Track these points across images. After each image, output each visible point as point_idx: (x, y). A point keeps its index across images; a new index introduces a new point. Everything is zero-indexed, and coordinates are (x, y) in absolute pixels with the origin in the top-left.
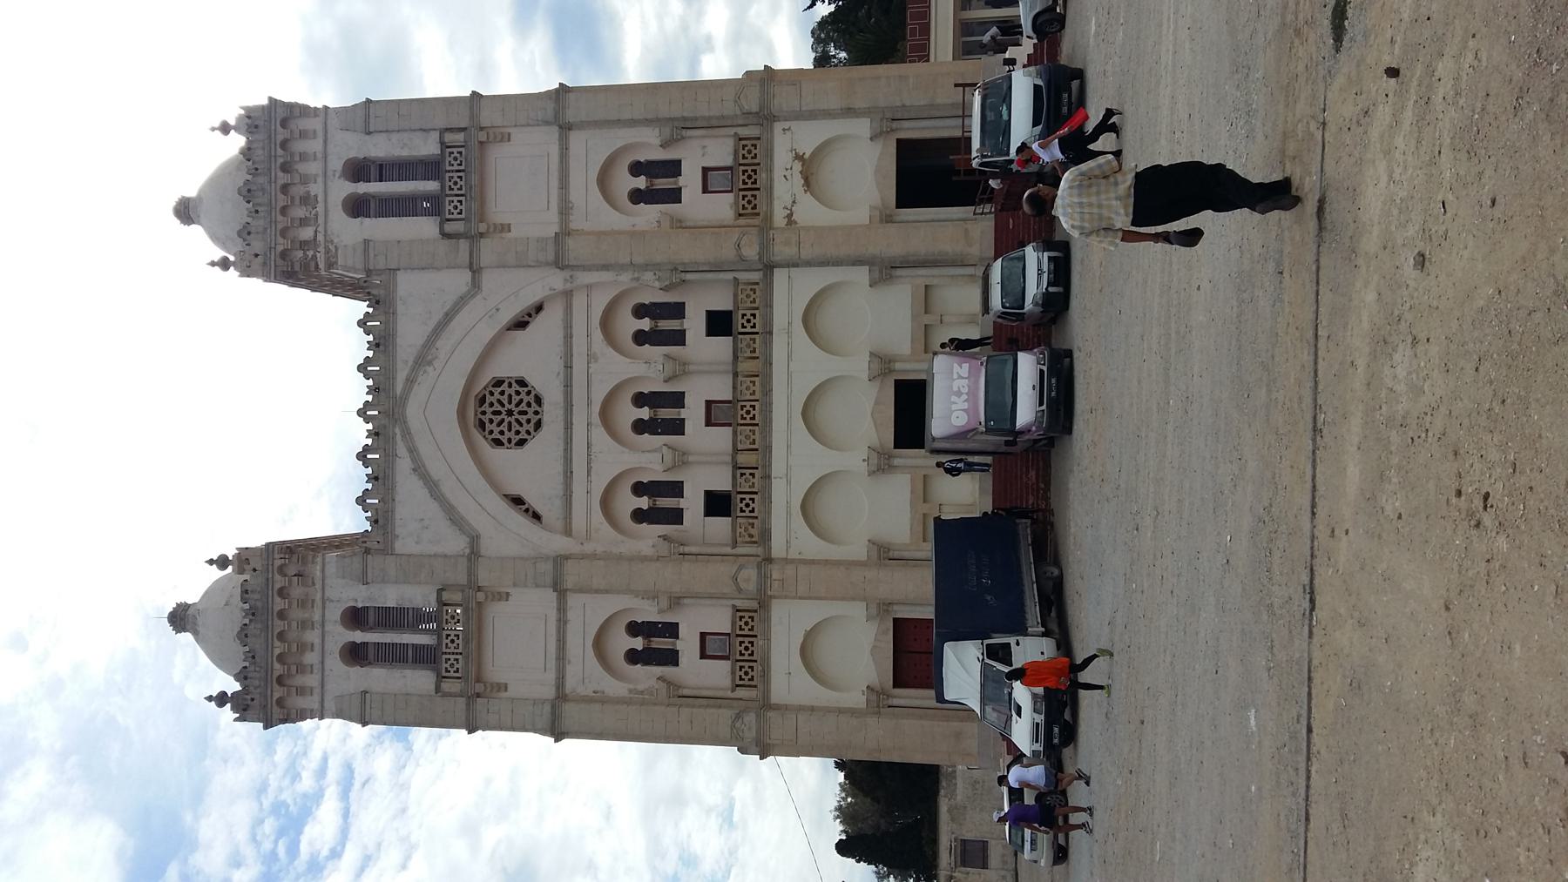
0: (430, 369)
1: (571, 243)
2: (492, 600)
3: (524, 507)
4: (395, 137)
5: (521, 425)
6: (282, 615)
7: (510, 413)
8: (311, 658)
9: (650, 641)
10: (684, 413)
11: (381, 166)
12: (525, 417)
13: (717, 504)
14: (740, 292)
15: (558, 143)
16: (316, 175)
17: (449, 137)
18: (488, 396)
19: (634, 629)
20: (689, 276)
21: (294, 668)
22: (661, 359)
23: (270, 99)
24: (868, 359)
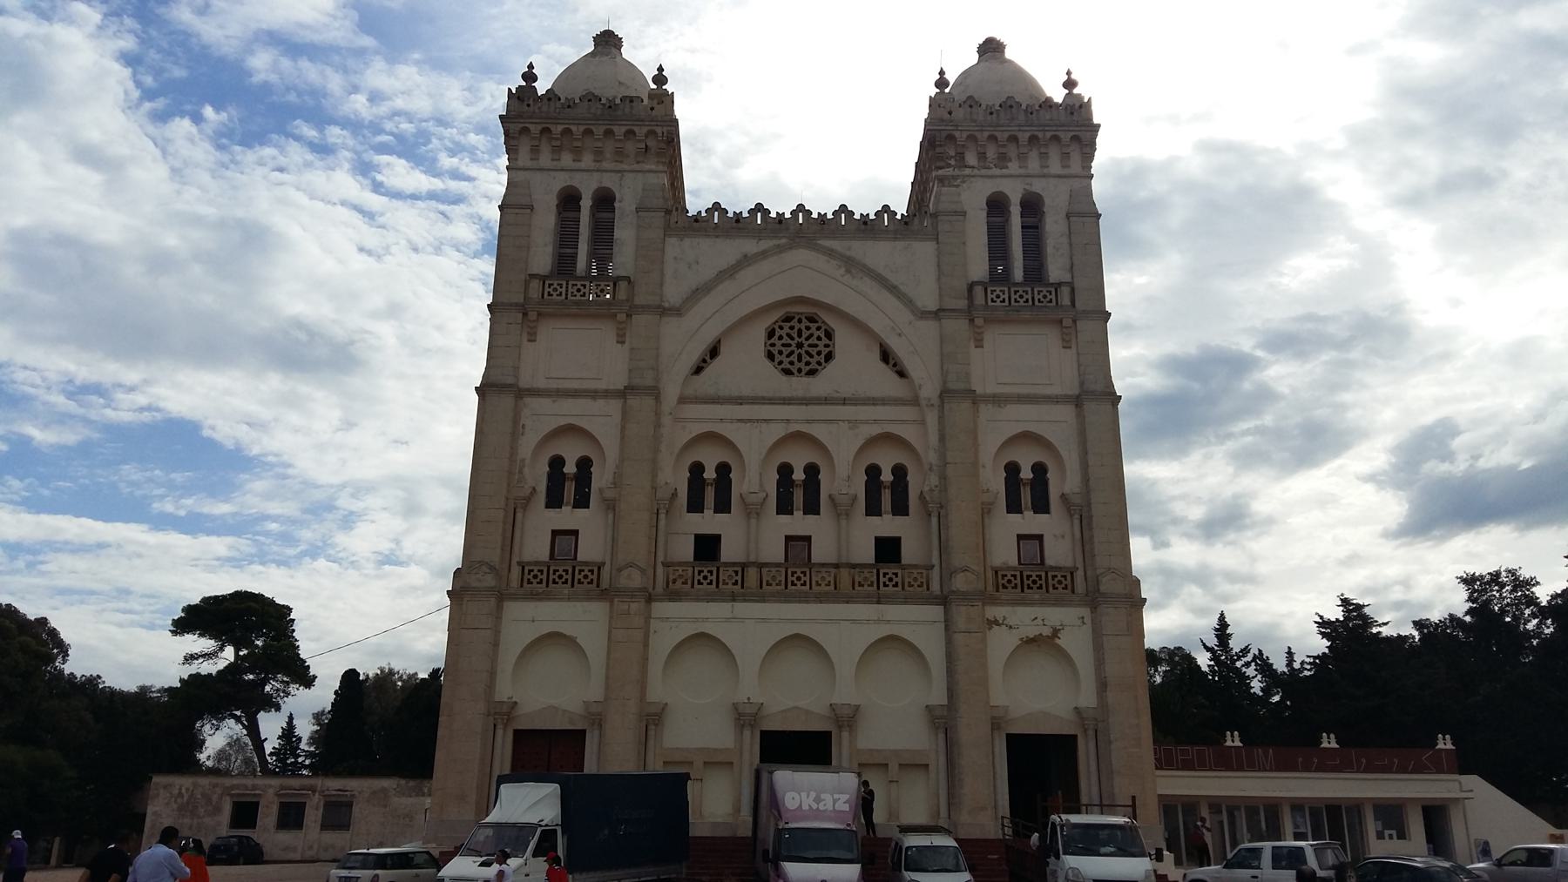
0: (842, 271)
1: (966, 405)
2: (618, 328)
3: (708, 358)
4: (1065, 240)
5: (788, 356)
6: (609, 133)
7: (800, 346)
8: (567, 159)
9: (572, 480)
10: (798, 514)
11: (1037, 227)
12: (796, 360)
13: (707, 547)
14: (919, 571)
15: (1064, 393)
16: (1026, 167)
17: (1065, 291)
18: (816, 325)
19: (585, 464)
20: (934, 520)
21: (558, 143)
22: (852, 492)
23: (1099, 126)
24: (853, 704)
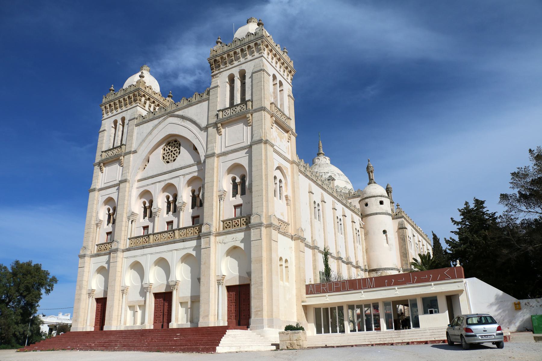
7: (172, 151)
